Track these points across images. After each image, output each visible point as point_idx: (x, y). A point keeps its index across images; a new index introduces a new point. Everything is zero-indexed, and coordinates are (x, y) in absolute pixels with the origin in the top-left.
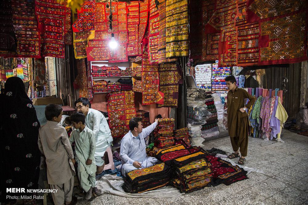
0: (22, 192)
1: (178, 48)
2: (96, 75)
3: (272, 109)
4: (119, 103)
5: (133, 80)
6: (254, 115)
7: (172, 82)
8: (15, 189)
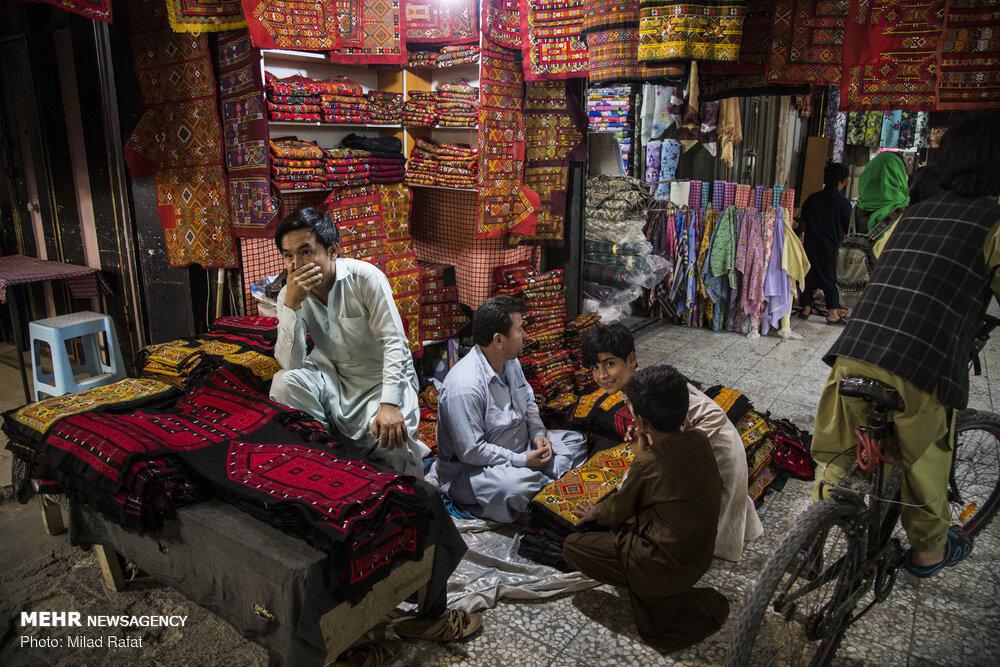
0: (70, 624)
1: (704, 27)
2: (282, 112)
3: (768, 245)
4: (363, 235)
5: (407, 140)
6: (717, 264)
7: (549, 152)
8: (48, 613)
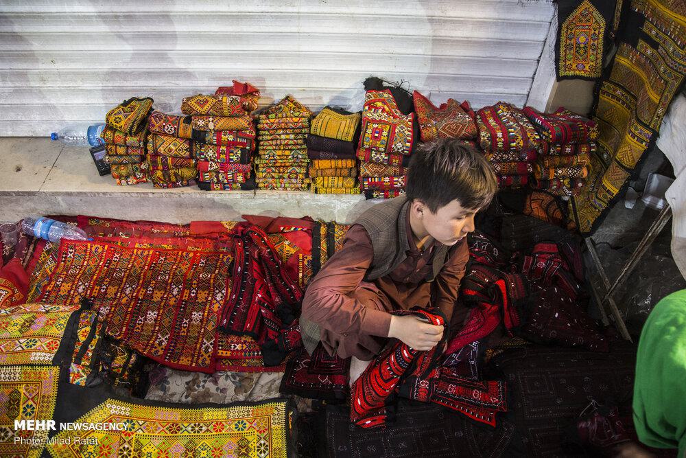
0: (49, 429)
8: (33, 421)
